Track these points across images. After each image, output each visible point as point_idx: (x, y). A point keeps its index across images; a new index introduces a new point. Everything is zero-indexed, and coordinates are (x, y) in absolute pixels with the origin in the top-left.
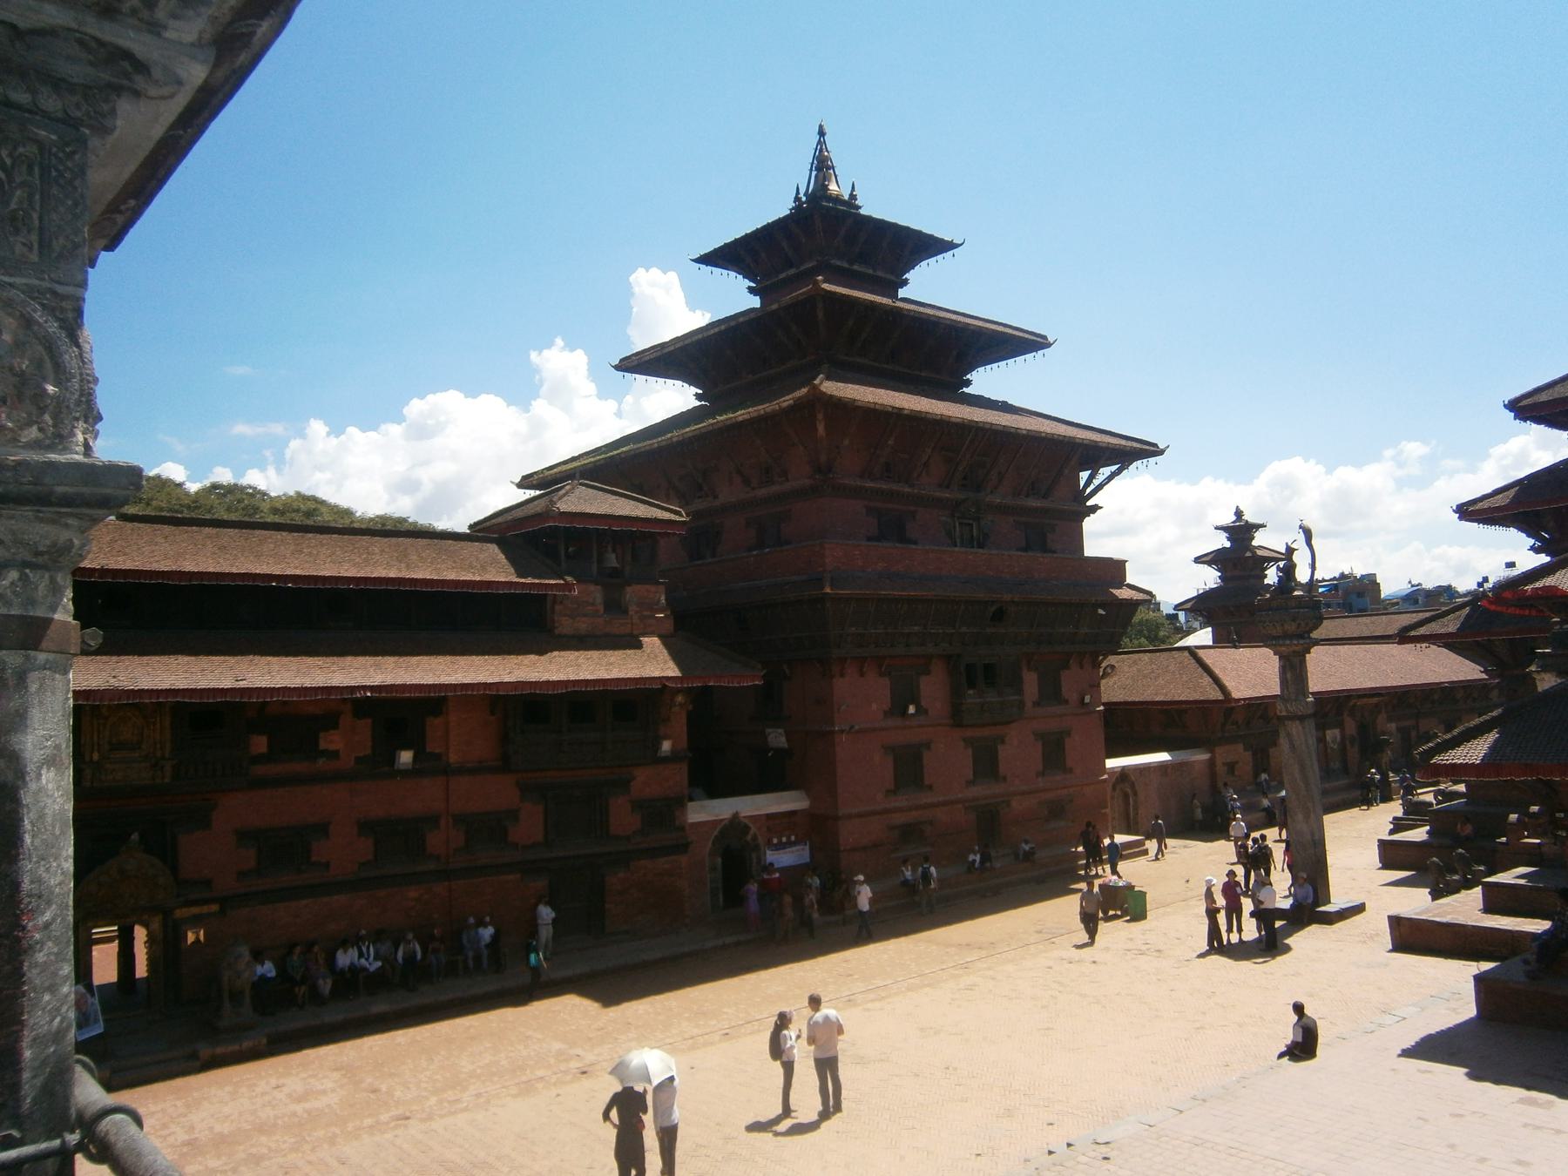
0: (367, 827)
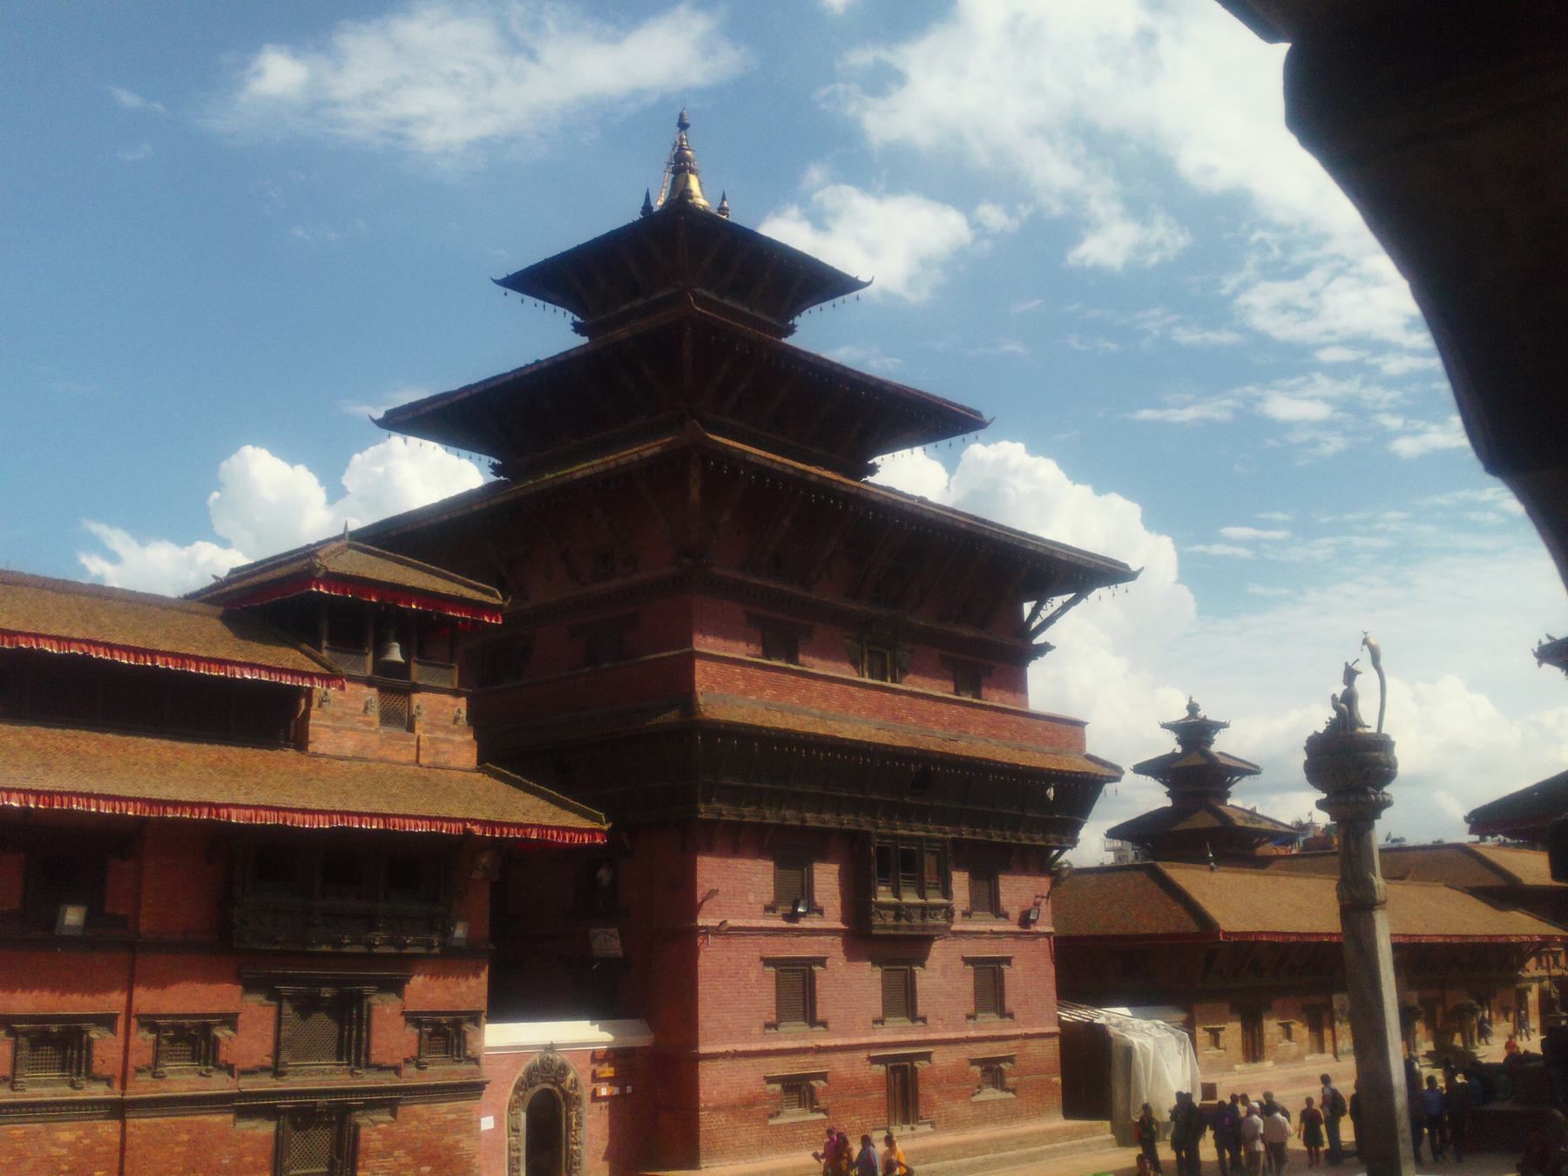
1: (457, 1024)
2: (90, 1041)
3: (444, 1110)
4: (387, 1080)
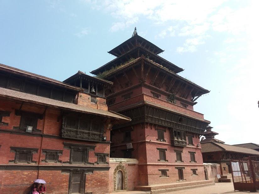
0: (13, 149)
1: (105, 156)
2: (32, 154)
3: (102, 172)
4: (92, 166)
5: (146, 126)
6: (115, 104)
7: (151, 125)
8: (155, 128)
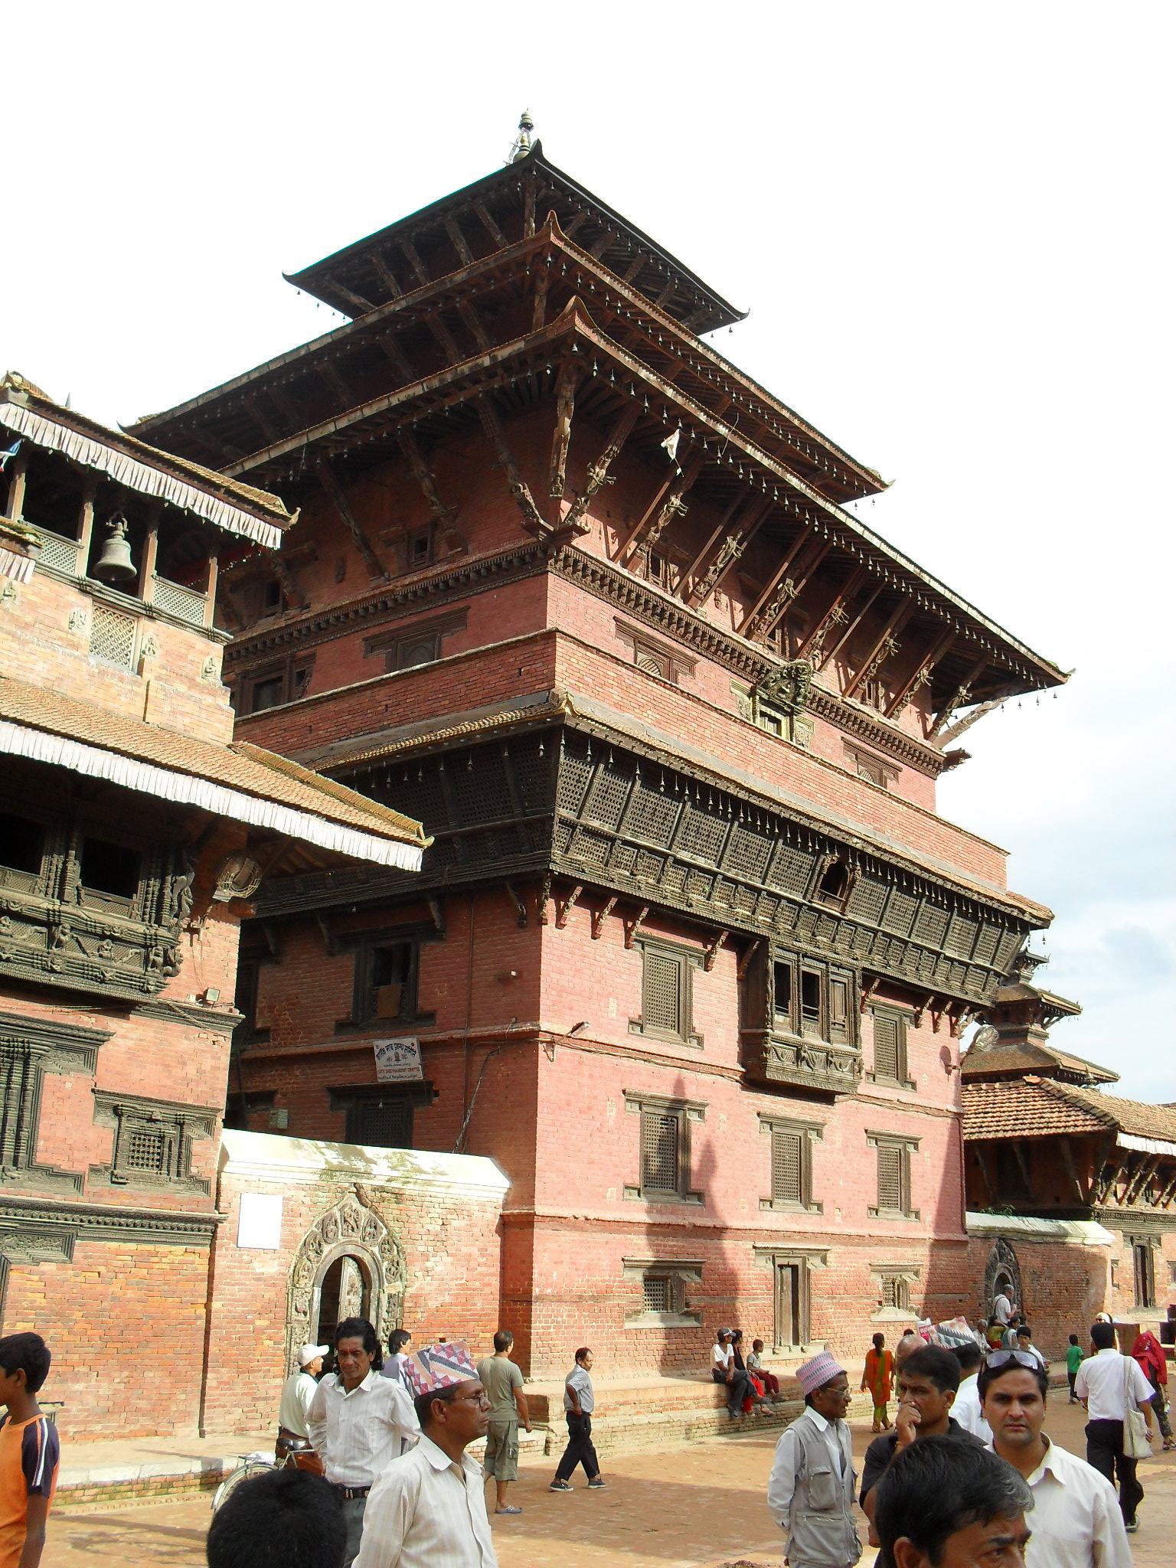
5: (550, 906)
6: (303, 706)
7: (595, 898)
8: (628, 932)
